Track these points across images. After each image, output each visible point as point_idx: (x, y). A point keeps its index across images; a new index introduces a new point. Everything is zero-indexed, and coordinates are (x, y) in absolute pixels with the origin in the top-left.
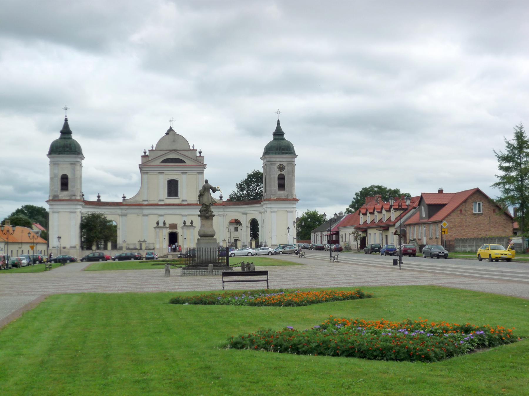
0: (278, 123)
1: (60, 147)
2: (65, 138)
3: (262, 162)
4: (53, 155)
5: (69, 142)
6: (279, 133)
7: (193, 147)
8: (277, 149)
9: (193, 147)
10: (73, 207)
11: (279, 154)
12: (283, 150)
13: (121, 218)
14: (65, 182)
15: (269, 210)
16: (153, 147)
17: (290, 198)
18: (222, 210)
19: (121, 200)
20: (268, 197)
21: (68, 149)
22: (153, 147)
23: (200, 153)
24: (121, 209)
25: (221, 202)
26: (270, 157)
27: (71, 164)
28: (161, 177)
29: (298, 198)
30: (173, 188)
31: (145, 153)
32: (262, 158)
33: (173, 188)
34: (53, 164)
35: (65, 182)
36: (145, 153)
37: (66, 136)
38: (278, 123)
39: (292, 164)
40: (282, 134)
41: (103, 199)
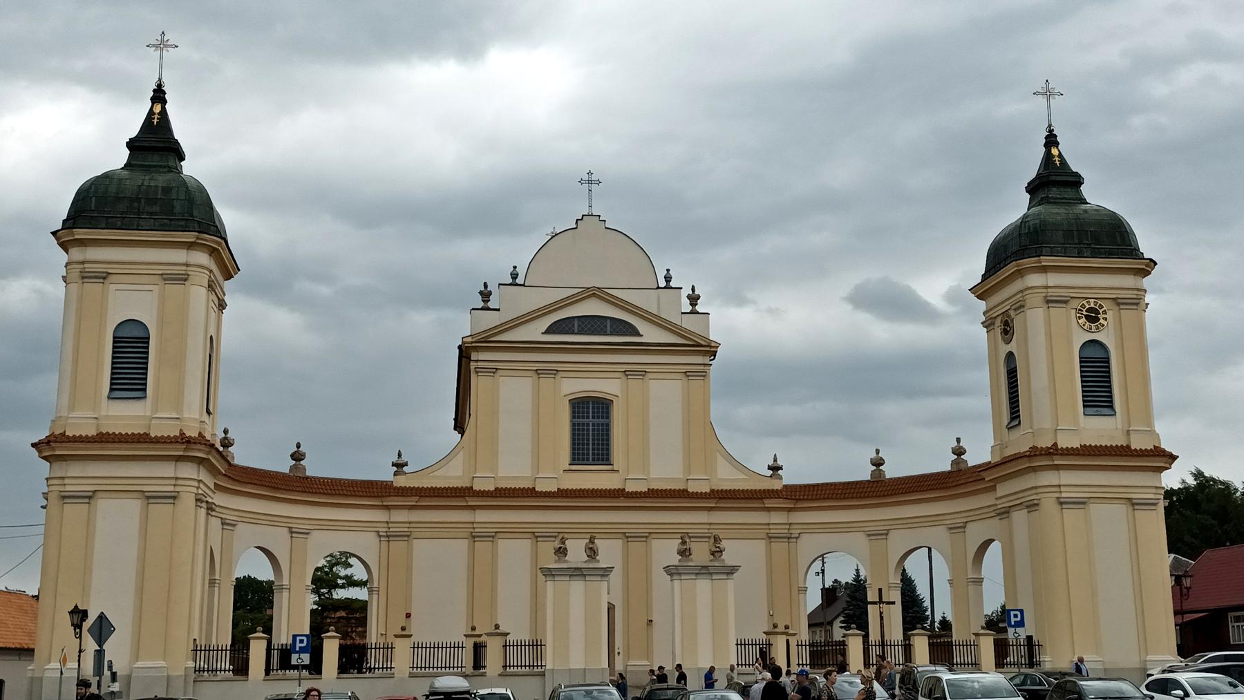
0: (1051, 140)
1: (118, 199)
2: (147, 169)
3: (982, 305)
4: (80, 233)
5: (161, 180)
6: (1054, 180)
7: (668, 279)
8: (1068, 234)
9: (668, 279)
10: (167, 469)
11: (1080, 255)
12: (1096, 238)
13: (384, 544)
14: (130, 359)
15: (1048, 504)
16: (514, 276)
17: (1137, 444)
18: (777, 518)
19: (385, 473)
20: (1045, 443)
21: (156, 209)
22: (514, 276)
23: (694, 299)
24: (388, 508)
25: (777, 485)
26: (1044, 269)
27: (168, 278)
28: (546, 382)
29: (1166, 446)
30: (591, 429)
31: (486, 295)
32: (981, 291)
33: (591, 429)
34: (85, 276)
35: (130, 359)
36: (486, 295)
37: (154, 159)
38: (1051, 140)
39: (1136, 302)
40: (1076, 181)
41: (314, 468)
